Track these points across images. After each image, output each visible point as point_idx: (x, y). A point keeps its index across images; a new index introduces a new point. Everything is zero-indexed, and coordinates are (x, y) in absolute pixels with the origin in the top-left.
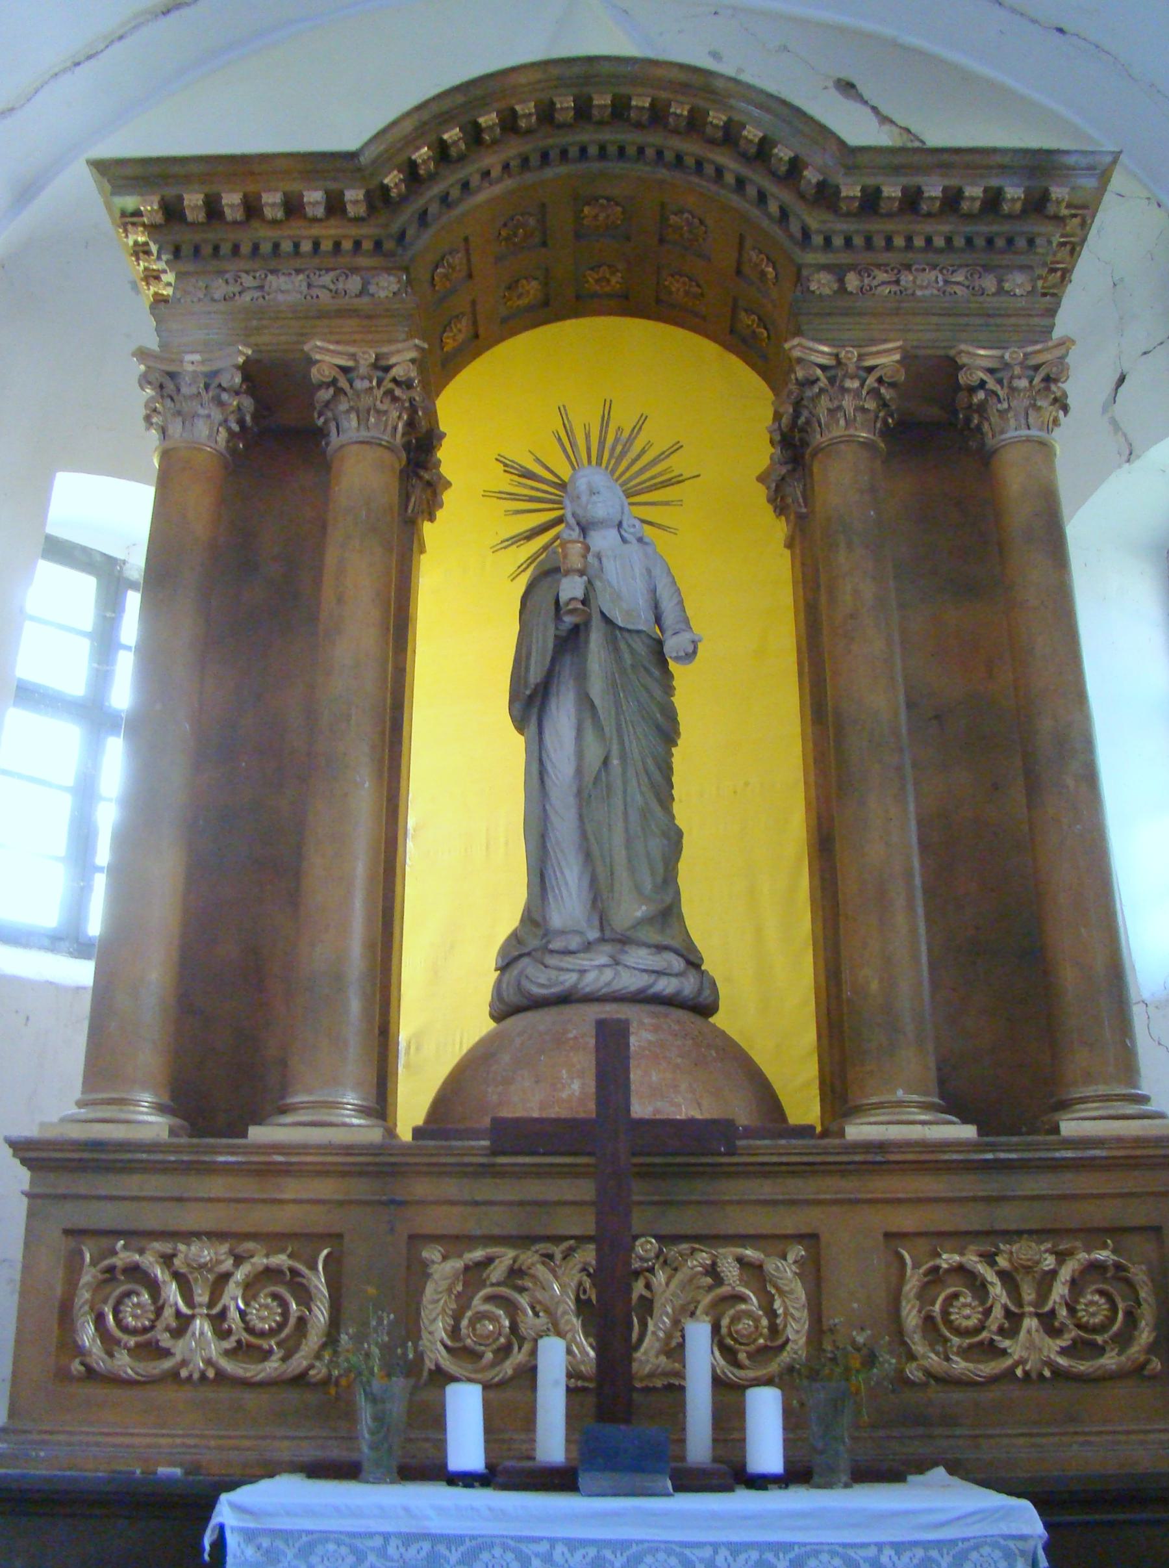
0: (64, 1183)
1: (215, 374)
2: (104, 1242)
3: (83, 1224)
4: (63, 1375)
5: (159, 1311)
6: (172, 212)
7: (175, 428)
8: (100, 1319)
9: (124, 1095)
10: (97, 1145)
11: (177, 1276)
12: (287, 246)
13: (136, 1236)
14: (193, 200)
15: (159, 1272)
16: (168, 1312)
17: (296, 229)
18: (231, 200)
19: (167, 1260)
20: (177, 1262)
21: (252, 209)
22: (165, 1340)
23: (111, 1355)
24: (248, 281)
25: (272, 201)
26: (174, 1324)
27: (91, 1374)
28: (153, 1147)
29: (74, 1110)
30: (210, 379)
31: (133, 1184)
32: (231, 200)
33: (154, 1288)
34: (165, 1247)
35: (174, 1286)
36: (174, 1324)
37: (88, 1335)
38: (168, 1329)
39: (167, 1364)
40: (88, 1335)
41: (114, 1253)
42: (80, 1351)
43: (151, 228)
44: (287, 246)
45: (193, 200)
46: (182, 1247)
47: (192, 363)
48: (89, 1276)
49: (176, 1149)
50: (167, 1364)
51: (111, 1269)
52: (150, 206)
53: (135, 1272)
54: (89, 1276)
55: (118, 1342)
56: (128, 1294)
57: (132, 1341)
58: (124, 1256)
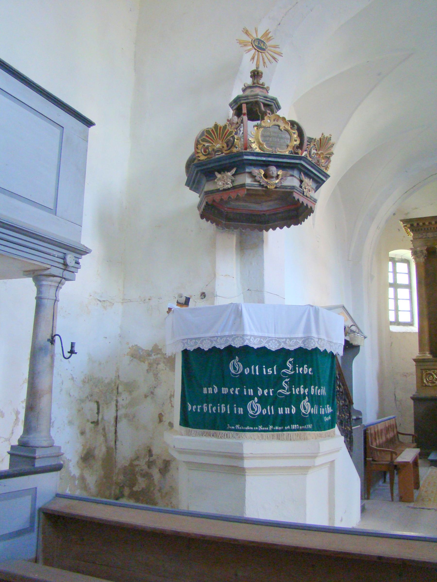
0: (421, 364)
1: (422, 250)
2: (426, 370)
3: (422, 368)
4: (423, 386)
5: (433, 378)
6: (412, 225)
7: (418, 260)
8: (426, 380)
9: (425, 353)
10: (424, 359)
11: (435, 374)
12: (429, 229)
13: (429, 370)
14: (415, 224)
15: (433, 374)
16: (435, 378)
17: (431, 226)
18: (421, 224)
19: (434, 372)
20: (435, 372)
21: (424, 224)
22: (435, 382)
23: (428, 383)
24: (424, 234)
25: (427, 223)
26: (435, 379)
27: (426, 386)
28: (431, 359)
29: (418, 355)
30: (421, 251)
31: (428, 363)
32: (421, 224)
33: (432, 375)
34: (433, 370)
35: (435, 375)
36: (435, 379)
37: (425, 381)
38: (435, 380)
39: (435, 384)
40: (425, 381)
41: (427, 371)
42: (425, 383)
43: (409, 228)
44: (429, 229)
45: (415, 224)
46: (435, 371)
47: (418, 249)
48: (424, 375)
49: (433, 359)
50: (435, 384)
51: (427, 374)
52: (409, 226)
53: (431, 374)
54: (424, 375)
55: (429, 382)
56: (429, 376)
57: (431, 382)
58: (429, 372)
